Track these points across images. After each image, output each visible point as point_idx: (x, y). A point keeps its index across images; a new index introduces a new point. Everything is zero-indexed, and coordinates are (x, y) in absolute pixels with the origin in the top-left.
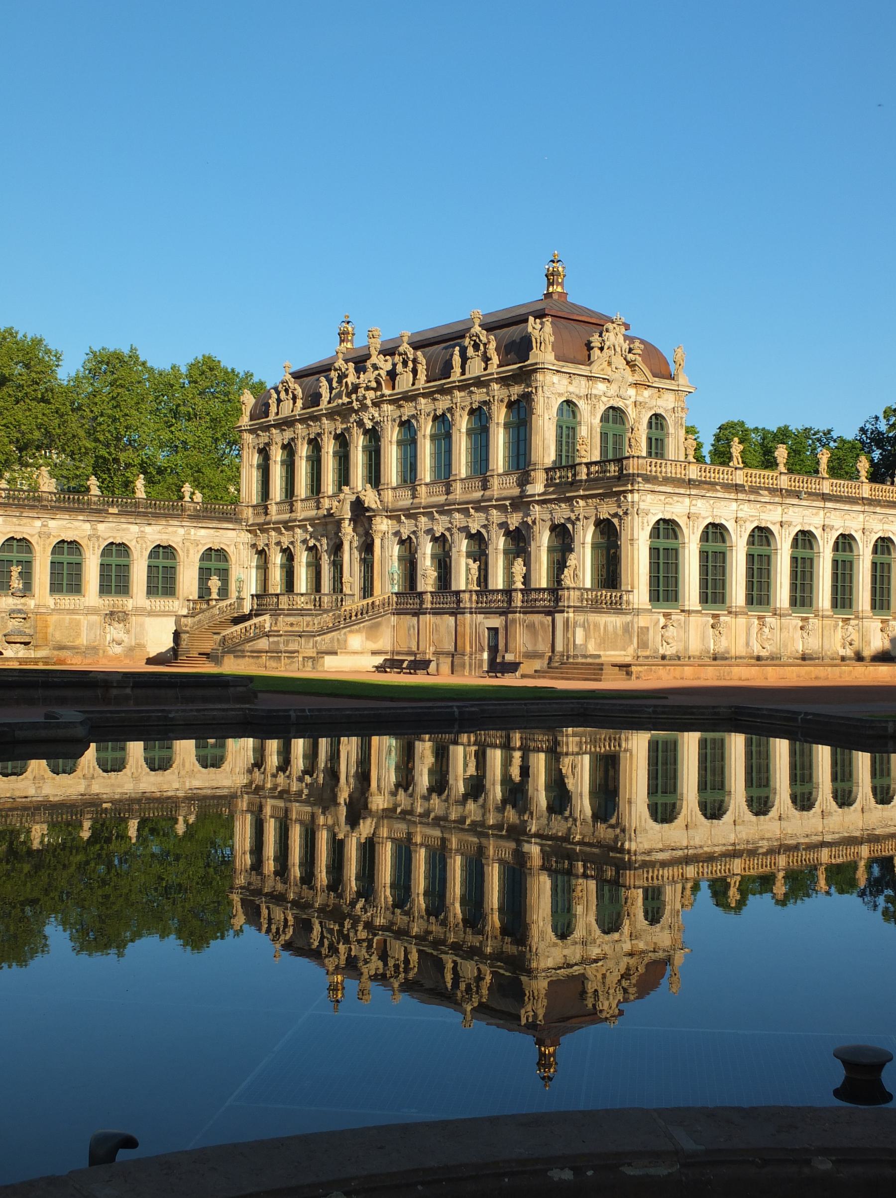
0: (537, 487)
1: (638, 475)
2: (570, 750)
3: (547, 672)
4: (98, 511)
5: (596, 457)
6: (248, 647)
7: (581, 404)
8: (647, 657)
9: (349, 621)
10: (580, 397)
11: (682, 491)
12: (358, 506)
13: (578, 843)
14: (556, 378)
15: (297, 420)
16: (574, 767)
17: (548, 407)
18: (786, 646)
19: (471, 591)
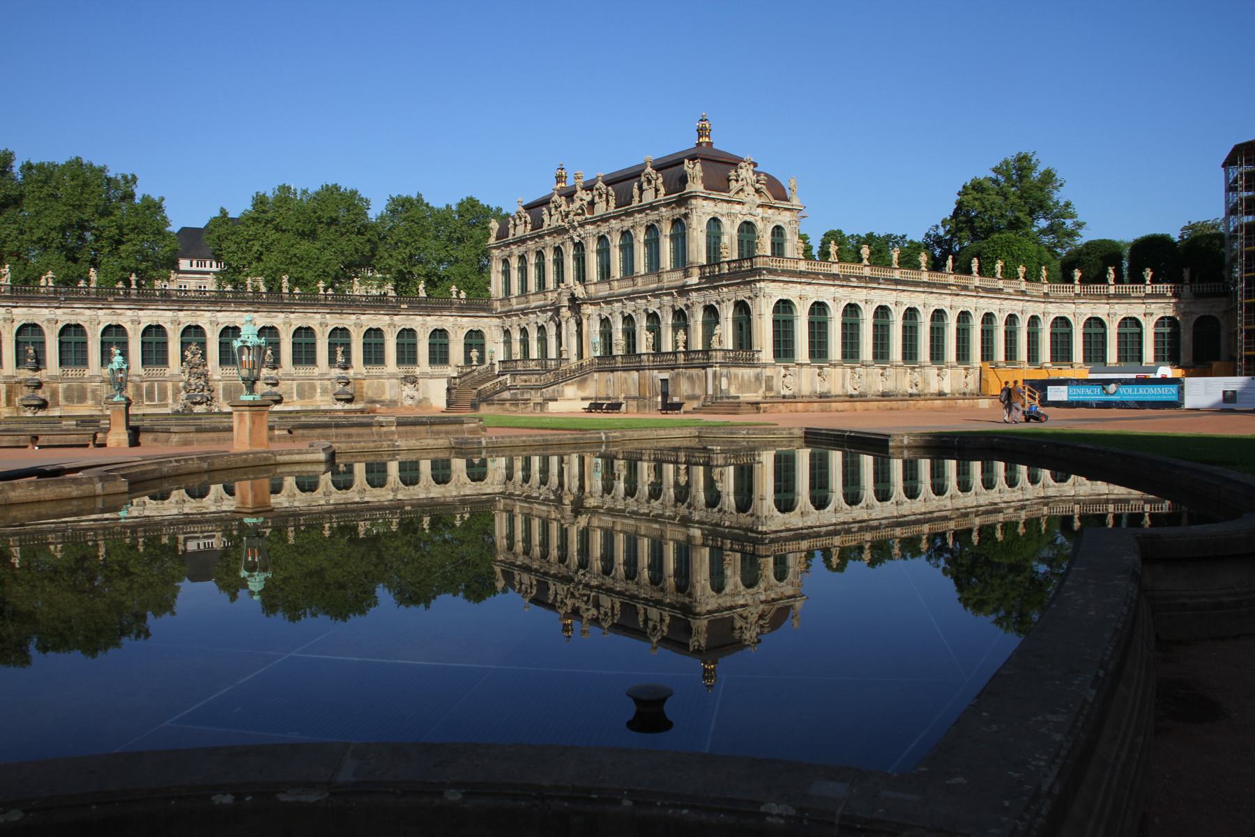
0: (694, 280)
1: (764, 269)
2: (719, 463)
3: (701, 409)
4: (394, 307)
5: (735, 257)
6: (496, 397)
7: (724, 220)
8: (772, 397)
9: (563, 377)
10: (723, 215)
11: (795, 280)
12: (573, 298)
13: (727, 527)
14: (705, 203)
15: (528, 239)
16: (722, 474)
17: (700, 223)
18: (870, 387)
19: (648, 354)
